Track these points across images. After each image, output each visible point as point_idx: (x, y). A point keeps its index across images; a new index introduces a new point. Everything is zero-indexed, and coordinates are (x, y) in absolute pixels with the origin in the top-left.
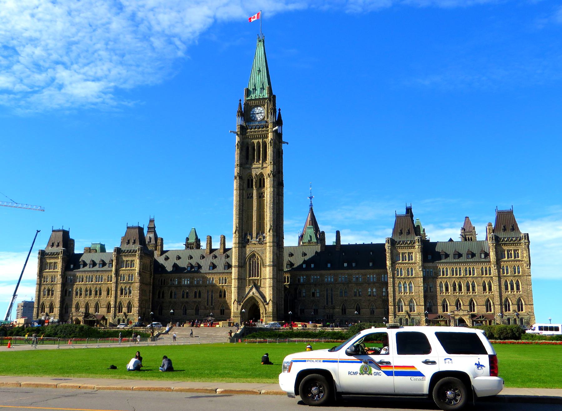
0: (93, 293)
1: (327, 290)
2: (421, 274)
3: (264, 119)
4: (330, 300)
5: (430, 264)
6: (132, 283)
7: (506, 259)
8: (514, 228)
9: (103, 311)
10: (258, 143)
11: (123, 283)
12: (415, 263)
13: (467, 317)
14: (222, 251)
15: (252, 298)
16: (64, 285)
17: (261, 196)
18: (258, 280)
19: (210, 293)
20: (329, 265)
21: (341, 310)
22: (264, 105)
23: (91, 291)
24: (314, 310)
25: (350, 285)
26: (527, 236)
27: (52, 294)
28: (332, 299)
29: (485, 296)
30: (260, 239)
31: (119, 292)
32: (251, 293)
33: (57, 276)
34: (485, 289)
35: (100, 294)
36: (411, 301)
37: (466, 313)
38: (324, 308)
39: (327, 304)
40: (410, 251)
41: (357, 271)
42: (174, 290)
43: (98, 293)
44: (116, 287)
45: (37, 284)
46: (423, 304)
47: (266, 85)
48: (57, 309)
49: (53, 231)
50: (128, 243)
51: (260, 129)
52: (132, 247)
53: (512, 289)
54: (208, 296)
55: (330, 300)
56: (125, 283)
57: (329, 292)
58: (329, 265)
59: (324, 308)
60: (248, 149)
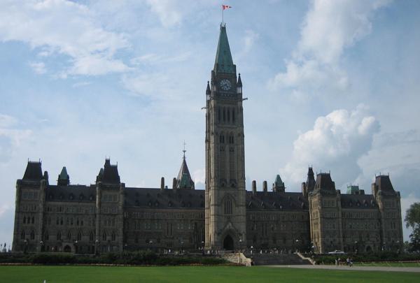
0: (75, 221)
5: (344, 210)
6: (115, 215)
9: (85, 239)
10: (229, 108)
17: (232, 150)
19: (170, 225)
21: (272, 241)
23: (72, 221)
27: (33, 222)
31: (102, 222)
32: (228, 227)
33: (38, 205)
42: (137, 221)
56: (108, 215)
57: (264, 227)
60: (219, 111)
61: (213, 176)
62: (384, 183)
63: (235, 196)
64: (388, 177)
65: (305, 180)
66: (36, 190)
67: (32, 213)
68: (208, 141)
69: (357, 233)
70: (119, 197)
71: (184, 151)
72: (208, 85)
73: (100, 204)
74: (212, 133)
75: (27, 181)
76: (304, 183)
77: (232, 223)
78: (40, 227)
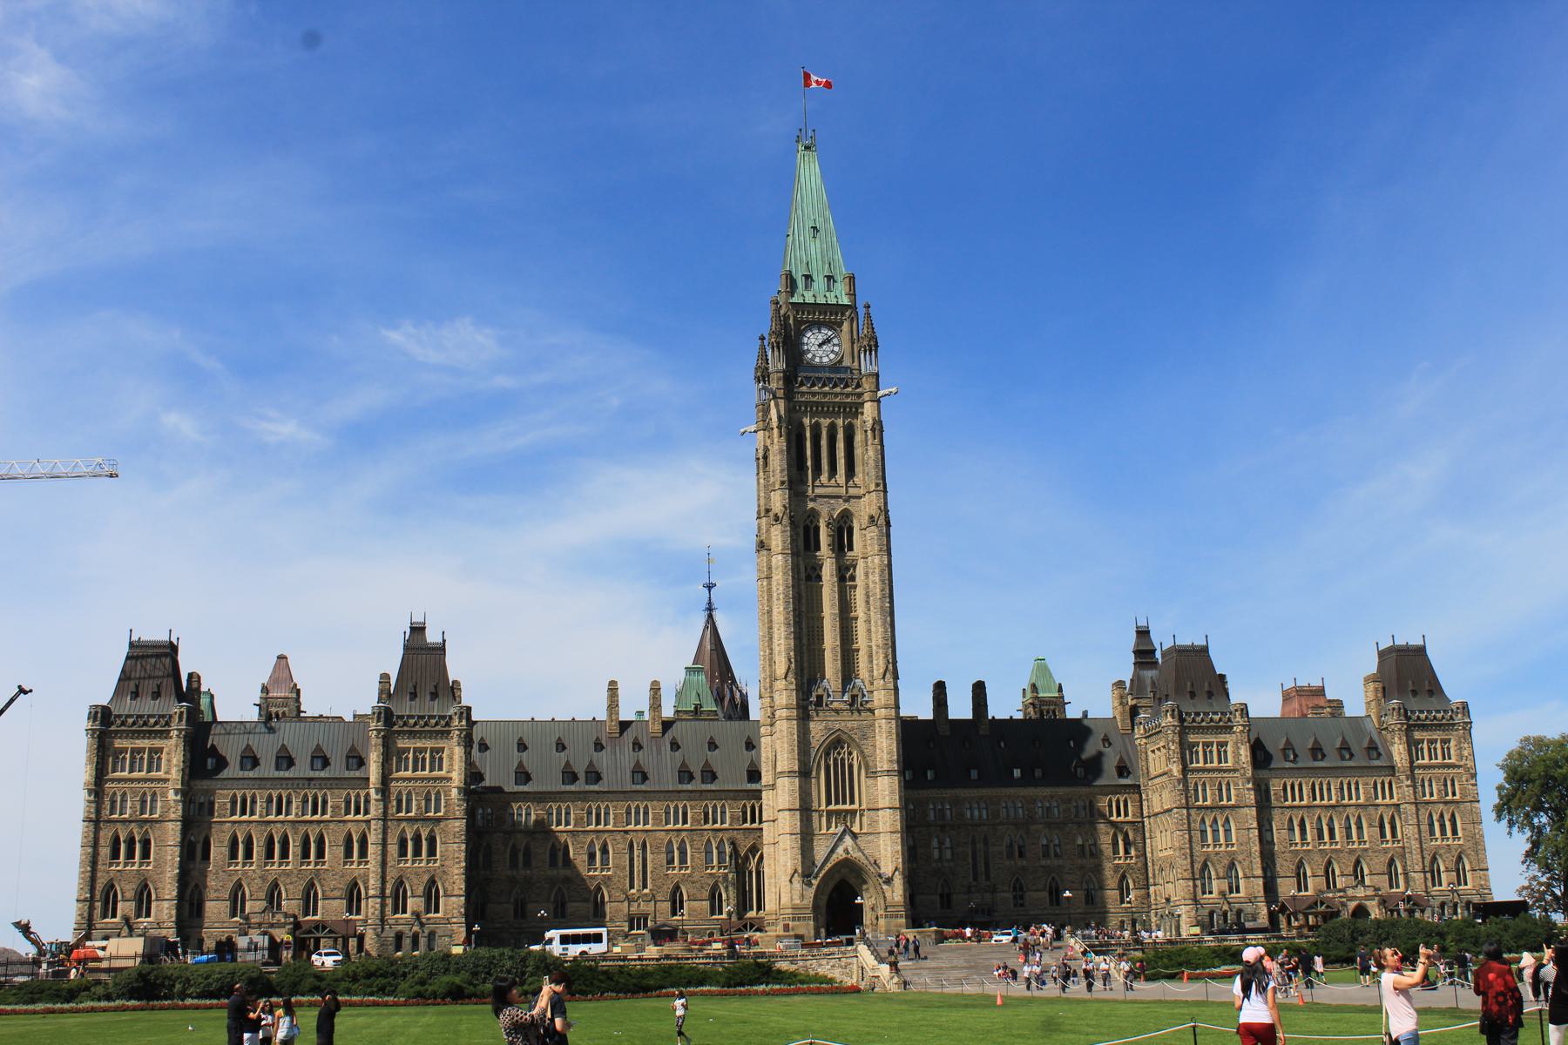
1: (974, 843)
2: (1251, 797)
3: (840, 361)
4: (981, 868)
6: (439, 820)
7: (1440, 760)
8: (1435, 689)
9: (330, 909)
11: (409, 820)
12: (1235, 770)
13: (1375, 903)
14: (658, 727)
15: (848, 864)
16: (187, 824)
17: (845, 574)
18: (853, 812)
20: (974, 774)
21: (1009, 895)
22: (840, 324)
24: (941, 896)
25: (1033, 827)
26: (1465, 707)
27: (146, 854)
28: (987, 865)
29: (1386, 851)
30: (854, 697)
31: (393, 849)
32: (840, 850)
33: (164, 795)
34: (1383, 835)
35: (320, 854)
36: (1232, 866)
37: (1370, 892)
38: (969, 892)
39: (975, 879)
40: (1222, 738)
41: (1047, 791)
43: (313, 848)
44: (385, 833)
45: (87, 820)
46: (1259, 872)
47: (841, 272)
48: (166, 904)
49: (132, 645)
50: (414, 696)
51: (838, 390)
52: (147, 706)
53: (1443, 831)
54: (631, 860)
55: (981, 868)
57: (980, 846)
58: (974, 774)
59: (969, 892)
61: (781, 669)
62: (1406, 673)
63: (864, 737)
64: (1421, 651)
65: (1126, 672)
66: (157, 743)
67: (146, 821)
68: (762, 546)
69: (1317, 857)
70: (451, 758)
71: (710, 587)
72: (763, 348)
73: (385, 780)
74: (777, 518)
75: (128, 706)
76: (1119, 684)
77: (855, 836)
78: (171, 872)
